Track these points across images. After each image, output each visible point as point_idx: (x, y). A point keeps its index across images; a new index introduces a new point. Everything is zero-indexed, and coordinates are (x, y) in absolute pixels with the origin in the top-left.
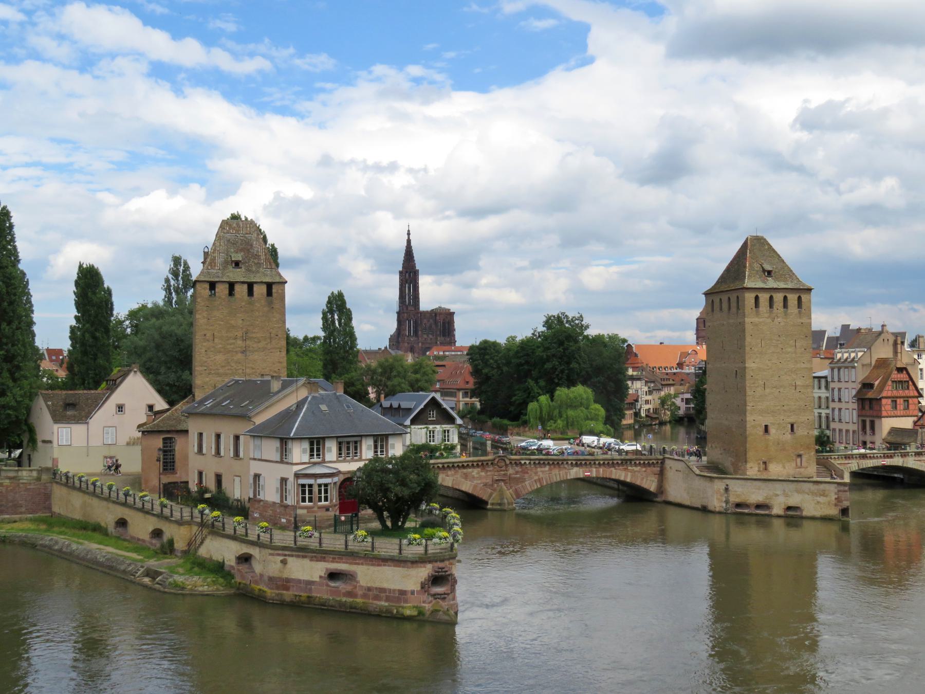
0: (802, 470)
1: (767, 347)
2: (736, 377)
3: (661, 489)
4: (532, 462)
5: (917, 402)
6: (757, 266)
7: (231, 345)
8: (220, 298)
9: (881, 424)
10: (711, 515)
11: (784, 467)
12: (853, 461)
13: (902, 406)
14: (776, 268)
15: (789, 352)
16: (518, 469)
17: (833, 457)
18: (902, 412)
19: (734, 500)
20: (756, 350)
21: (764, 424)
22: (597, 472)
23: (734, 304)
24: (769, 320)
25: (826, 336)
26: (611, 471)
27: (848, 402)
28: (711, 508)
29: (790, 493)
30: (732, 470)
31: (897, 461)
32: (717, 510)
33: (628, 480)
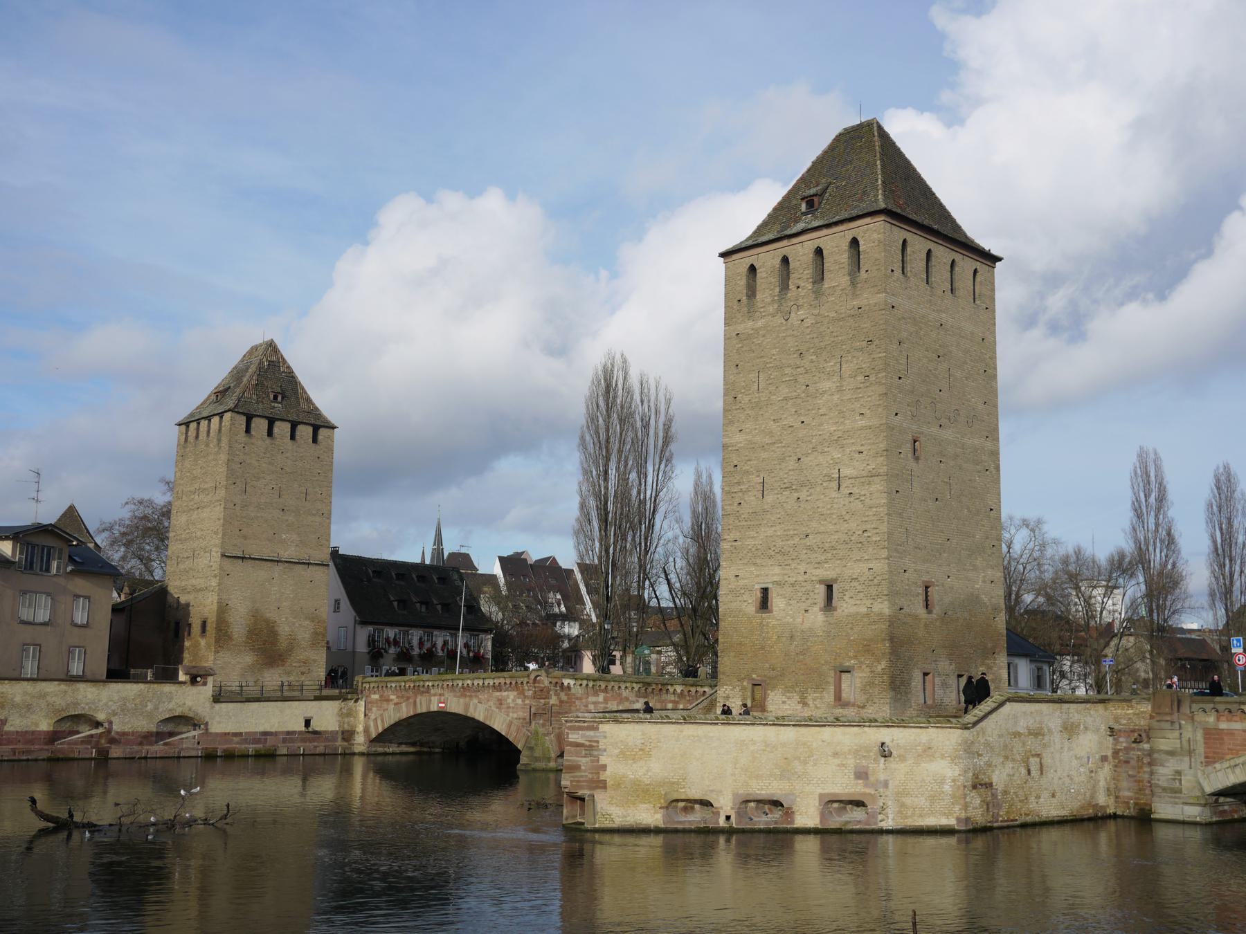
1: (772, 388)
8: (190, 442)
11: (805, 704)
15: (824, 392)
16: (563, 696)
20: (747, 399)
21: (758, 587)
24: (779, 320)
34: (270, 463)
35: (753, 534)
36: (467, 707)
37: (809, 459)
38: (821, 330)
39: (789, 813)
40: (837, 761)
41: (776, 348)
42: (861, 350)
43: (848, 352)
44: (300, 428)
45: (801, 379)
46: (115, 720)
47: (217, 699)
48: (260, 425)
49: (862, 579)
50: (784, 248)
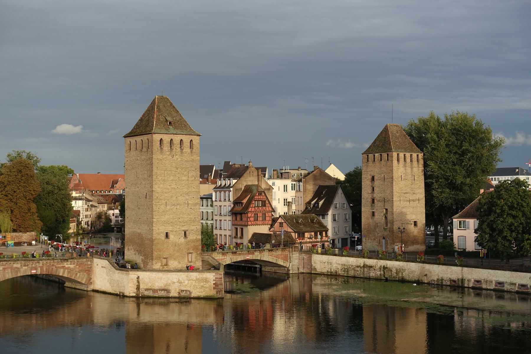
2: (146, 198)
3: (90, 281)
5: (271, 215)
6: (162, 118)
9: (248, 230)
10: (125, 298)
11: (180, 263)
12: (228, 257)
13: (261, 218)
14: (175, 120)
15: (184, 180)
18: (261, 222)
19: (143, 287)
20: (161, 178)
21: (165, 232)
22: (42, 268)
23: (145, 145)
24: (170, 157)
25: (214, 169)
26: (52, 268)
27: (226, 215)
28: (127, 294)
29: (183, 282)
30: (142, 266)
31: (257, 256)
32: (131, 295)
33: (66, 275)
35: (163, 217)
38: (183, 163)
41: (169, 165)
42: (194, 170)
43: (190, 170)
45: (177, 175)
50: (172, 136)
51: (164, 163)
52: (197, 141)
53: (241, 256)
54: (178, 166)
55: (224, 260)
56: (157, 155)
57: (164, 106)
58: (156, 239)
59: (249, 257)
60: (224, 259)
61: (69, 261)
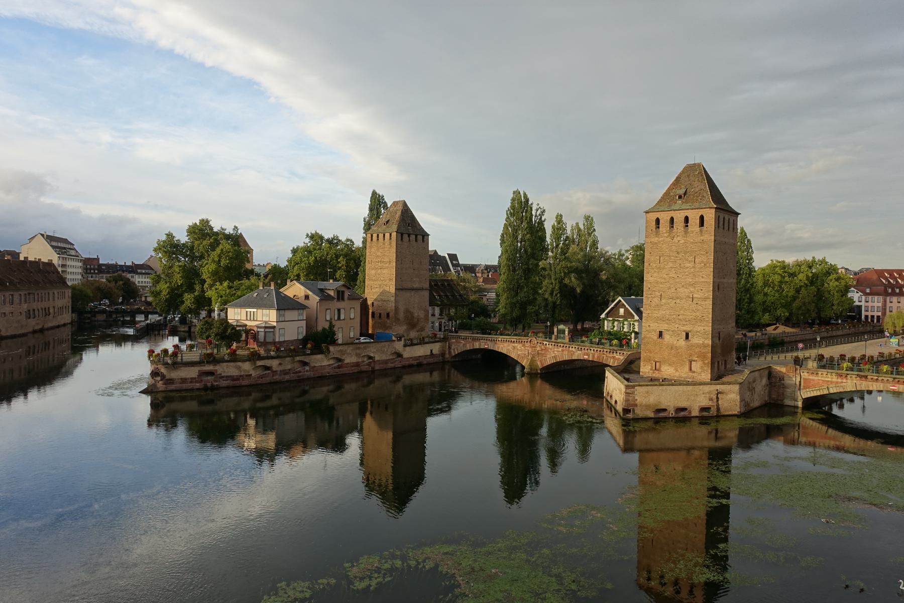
0: (695, 375)
4: (550, 344)
7: (377, 265)
11: (677, 370)
12: (848, 381)
16: (543, 347)
17: (820, 373)
20: (655, 265)
22: (593, 356)
26: (603, 357)
34: (410, 252)
36: (499, 348)
37: (681, 289)
39: (690, 412)
40: (704, 395)
44: (418, 236)
45: (678, 262)
46: (376, 356)
47: (405, 346)
48: (405, 236)
49: (701, 332)
50: (672, 214)
51: (661, 247)
52: (711, 215)
53: (878, 384)
54: (679, 250)
55: (842, 385)
56: (650, 238)
57: (688, 176)
58: (645, 337)
59: (896, 388)
60: (842, 382)
61: (618, 352)
